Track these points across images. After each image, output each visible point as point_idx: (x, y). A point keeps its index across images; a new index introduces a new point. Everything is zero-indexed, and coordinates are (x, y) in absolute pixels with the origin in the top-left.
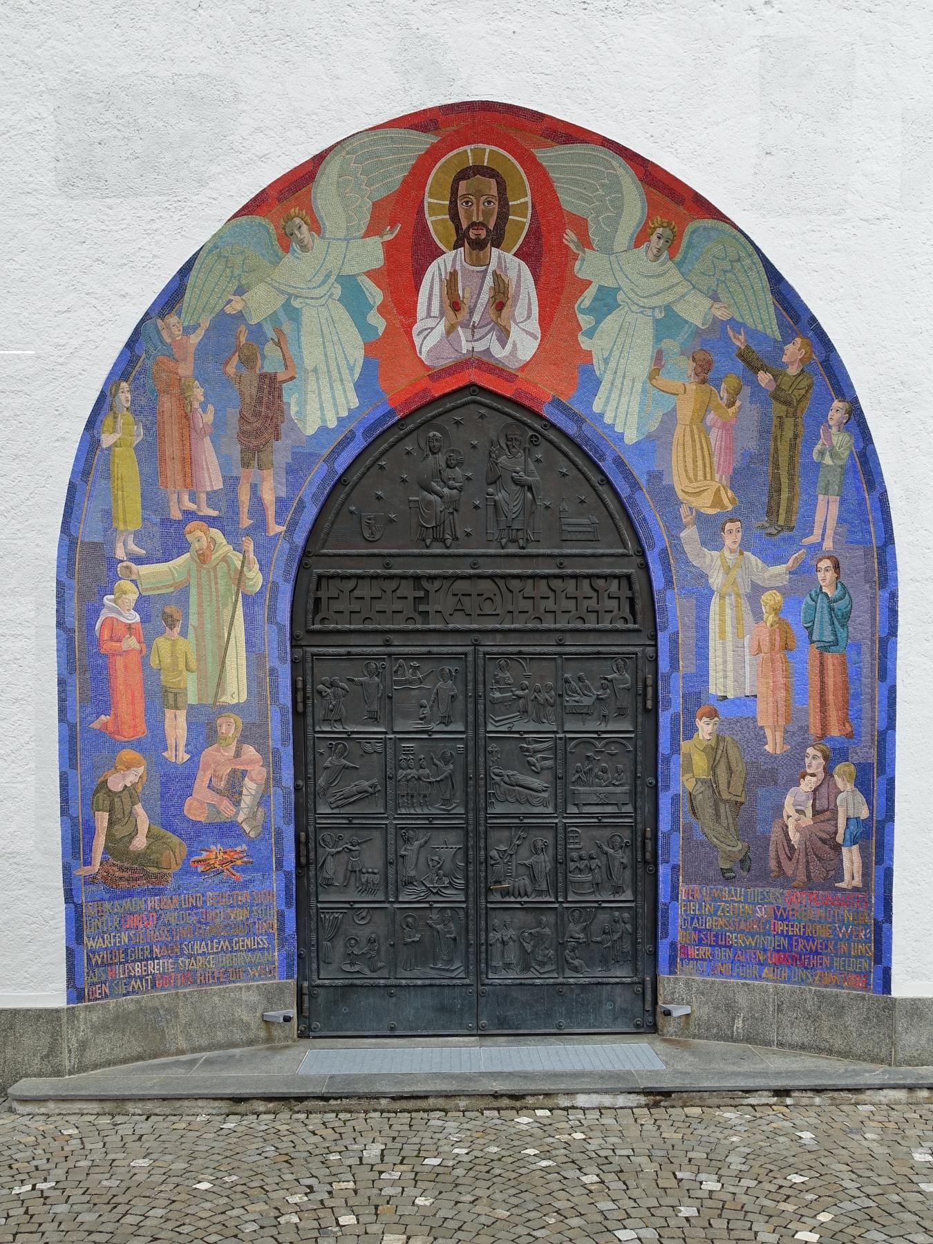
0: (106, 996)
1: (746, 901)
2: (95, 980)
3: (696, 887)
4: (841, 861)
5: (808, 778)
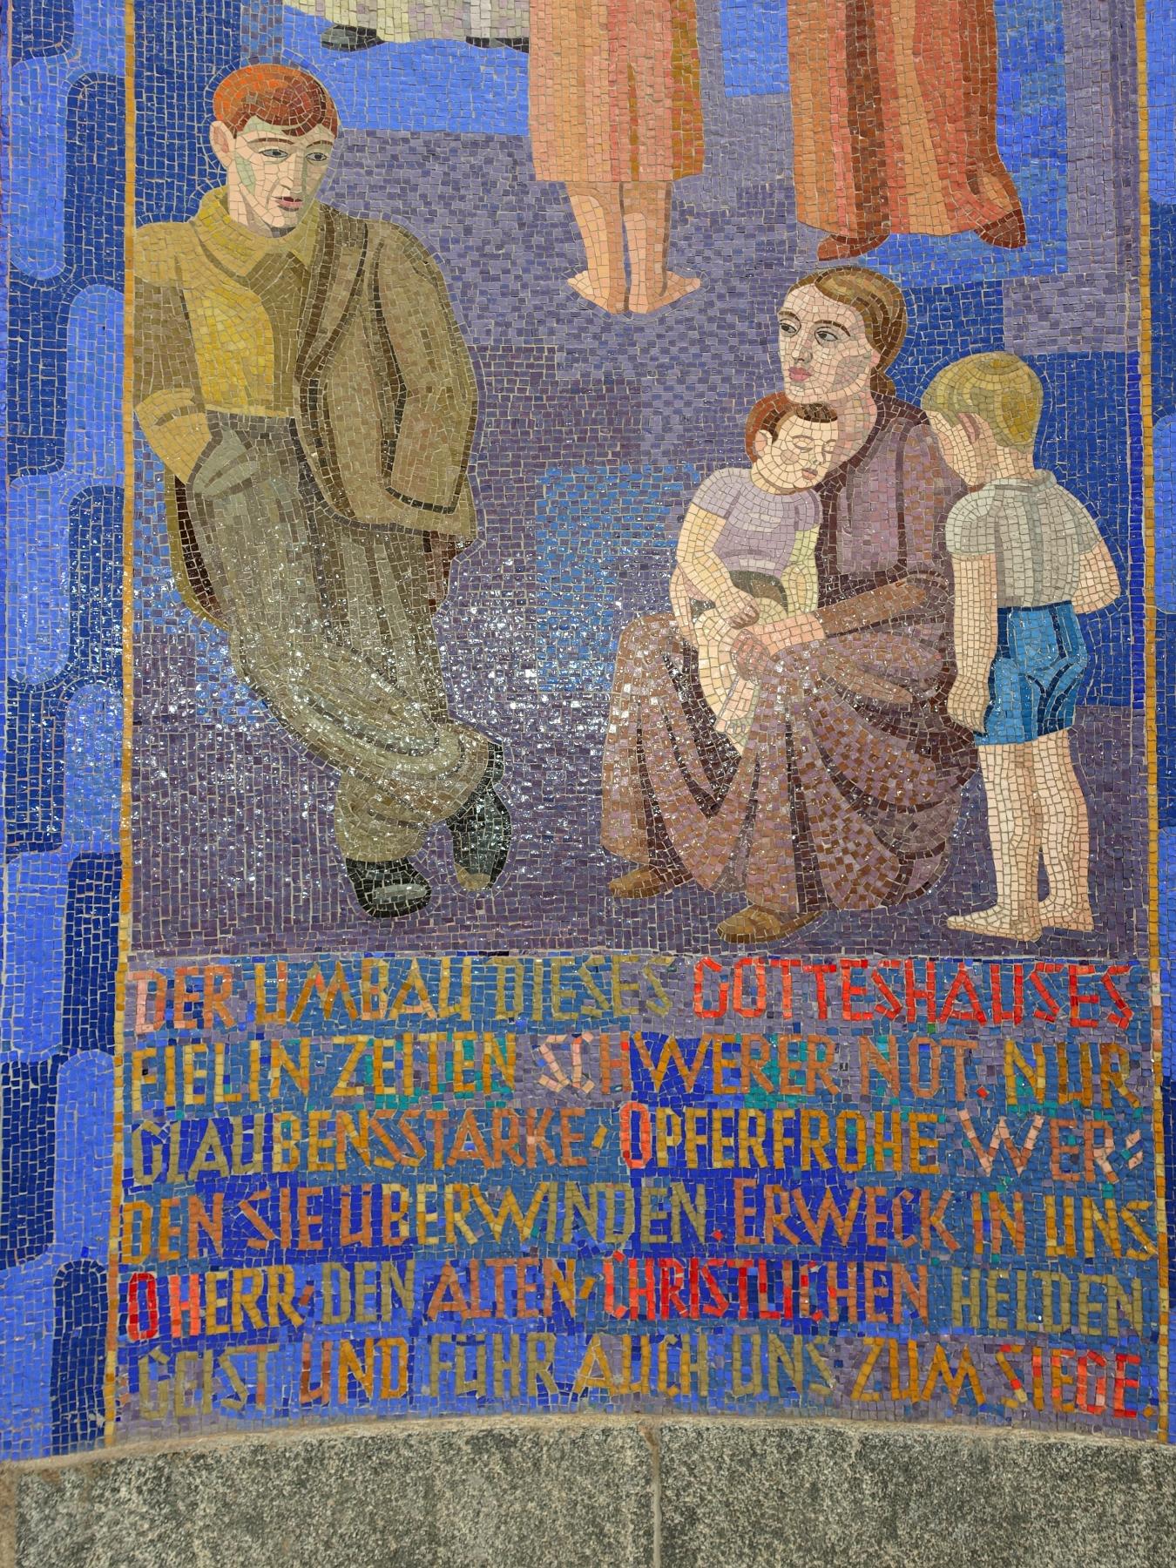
5: (793, 426)
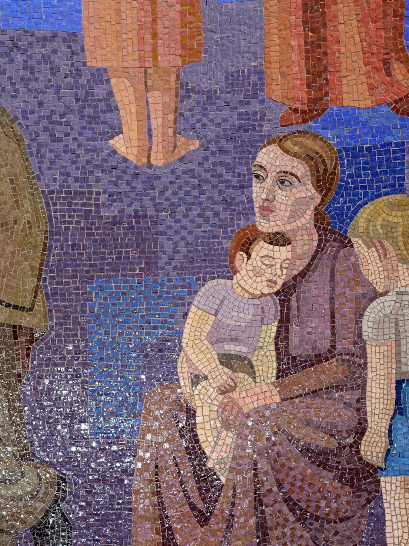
5: (261, 249)
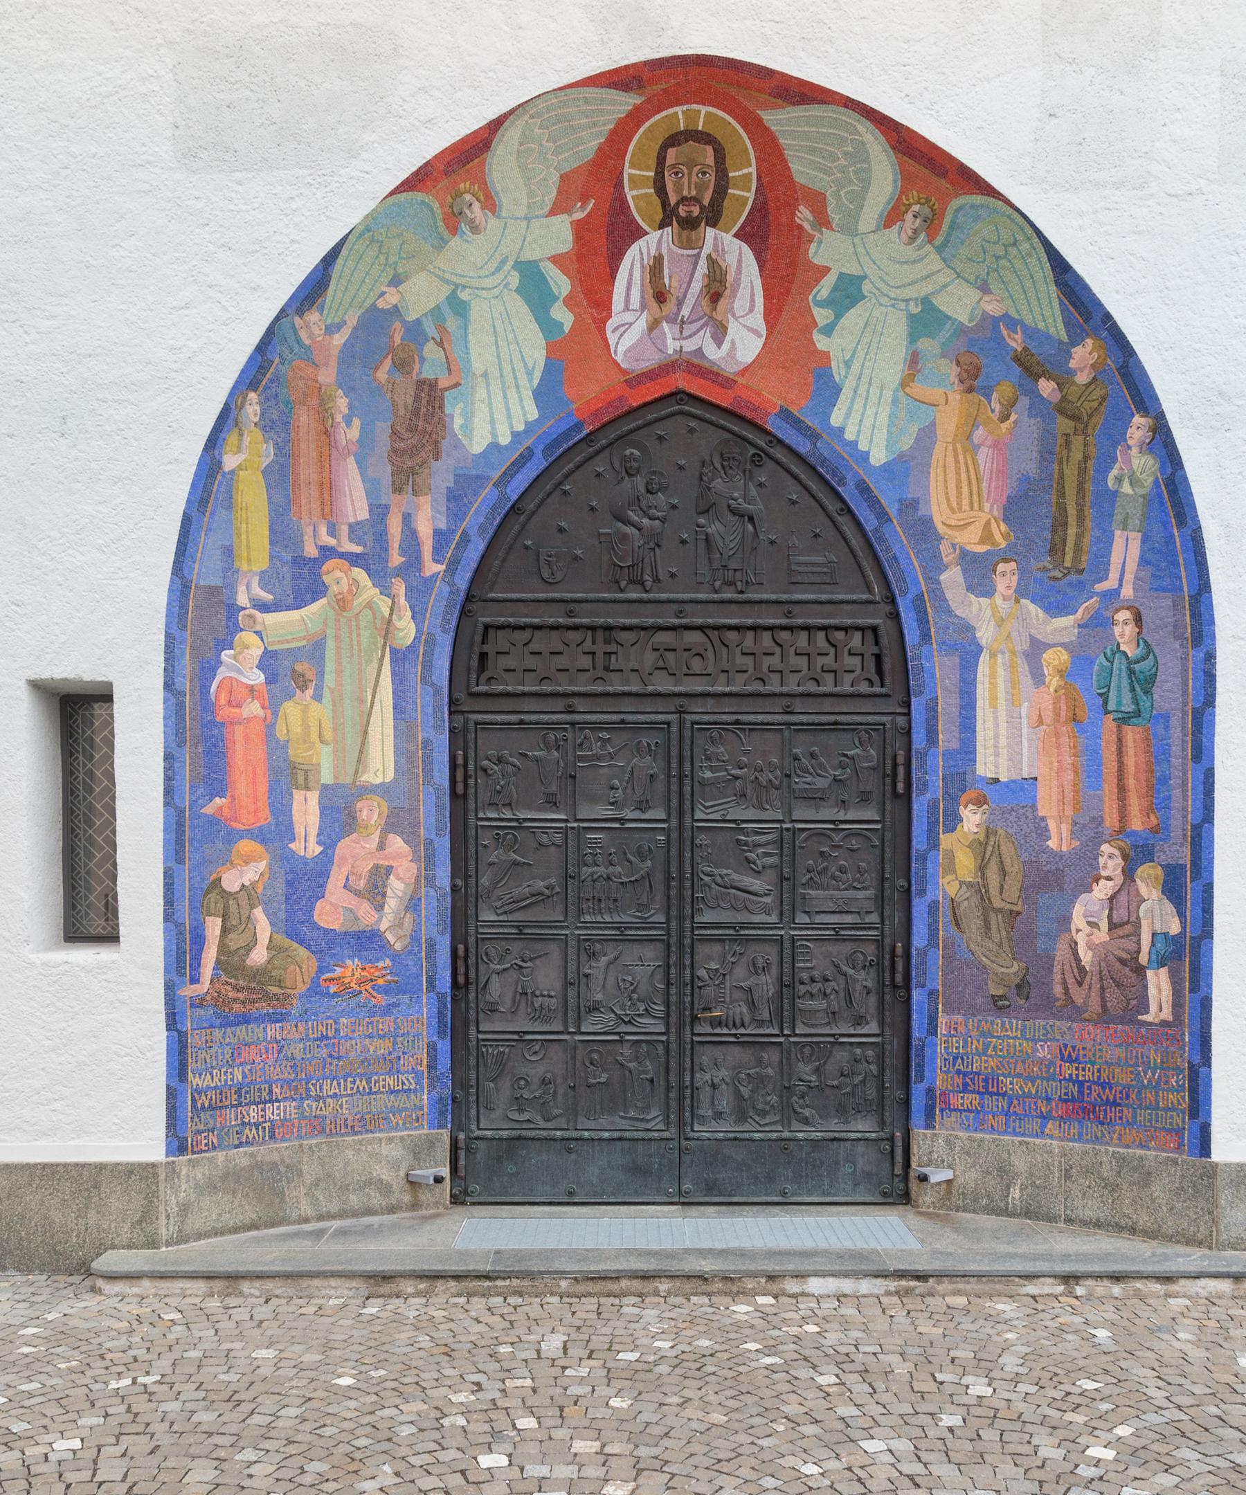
0: (214, 1148)
1: (1023, 1037)
2: (201, 1127)
3: (960, 1018)
4: (1146, 987)
5: (1102, 882)
